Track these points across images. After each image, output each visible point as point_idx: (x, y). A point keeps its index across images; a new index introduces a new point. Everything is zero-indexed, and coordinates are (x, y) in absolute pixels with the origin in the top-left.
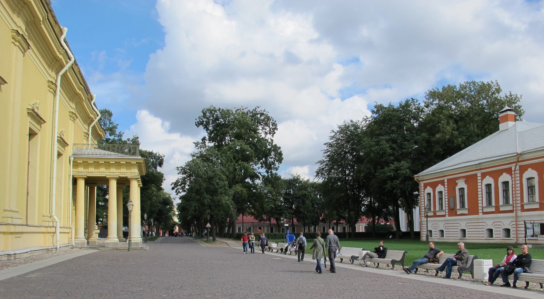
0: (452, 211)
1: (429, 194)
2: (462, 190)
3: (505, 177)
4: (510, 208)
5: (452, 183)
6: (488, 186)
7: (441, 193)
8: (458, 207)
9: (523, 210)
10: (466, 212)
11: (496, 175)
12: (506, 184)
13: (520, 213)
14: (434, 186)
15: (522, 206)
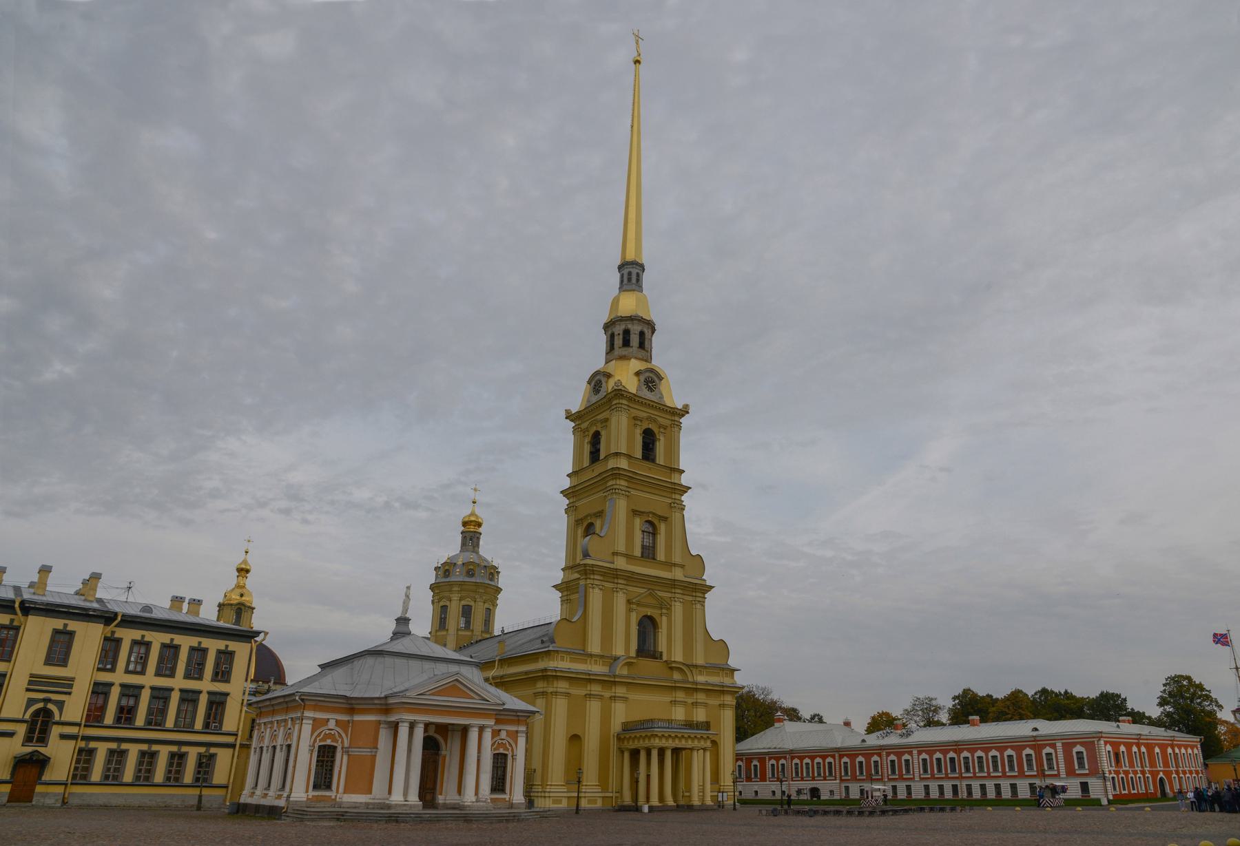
0: (749, 779)
3: (782, 761)
11: (777, 759)
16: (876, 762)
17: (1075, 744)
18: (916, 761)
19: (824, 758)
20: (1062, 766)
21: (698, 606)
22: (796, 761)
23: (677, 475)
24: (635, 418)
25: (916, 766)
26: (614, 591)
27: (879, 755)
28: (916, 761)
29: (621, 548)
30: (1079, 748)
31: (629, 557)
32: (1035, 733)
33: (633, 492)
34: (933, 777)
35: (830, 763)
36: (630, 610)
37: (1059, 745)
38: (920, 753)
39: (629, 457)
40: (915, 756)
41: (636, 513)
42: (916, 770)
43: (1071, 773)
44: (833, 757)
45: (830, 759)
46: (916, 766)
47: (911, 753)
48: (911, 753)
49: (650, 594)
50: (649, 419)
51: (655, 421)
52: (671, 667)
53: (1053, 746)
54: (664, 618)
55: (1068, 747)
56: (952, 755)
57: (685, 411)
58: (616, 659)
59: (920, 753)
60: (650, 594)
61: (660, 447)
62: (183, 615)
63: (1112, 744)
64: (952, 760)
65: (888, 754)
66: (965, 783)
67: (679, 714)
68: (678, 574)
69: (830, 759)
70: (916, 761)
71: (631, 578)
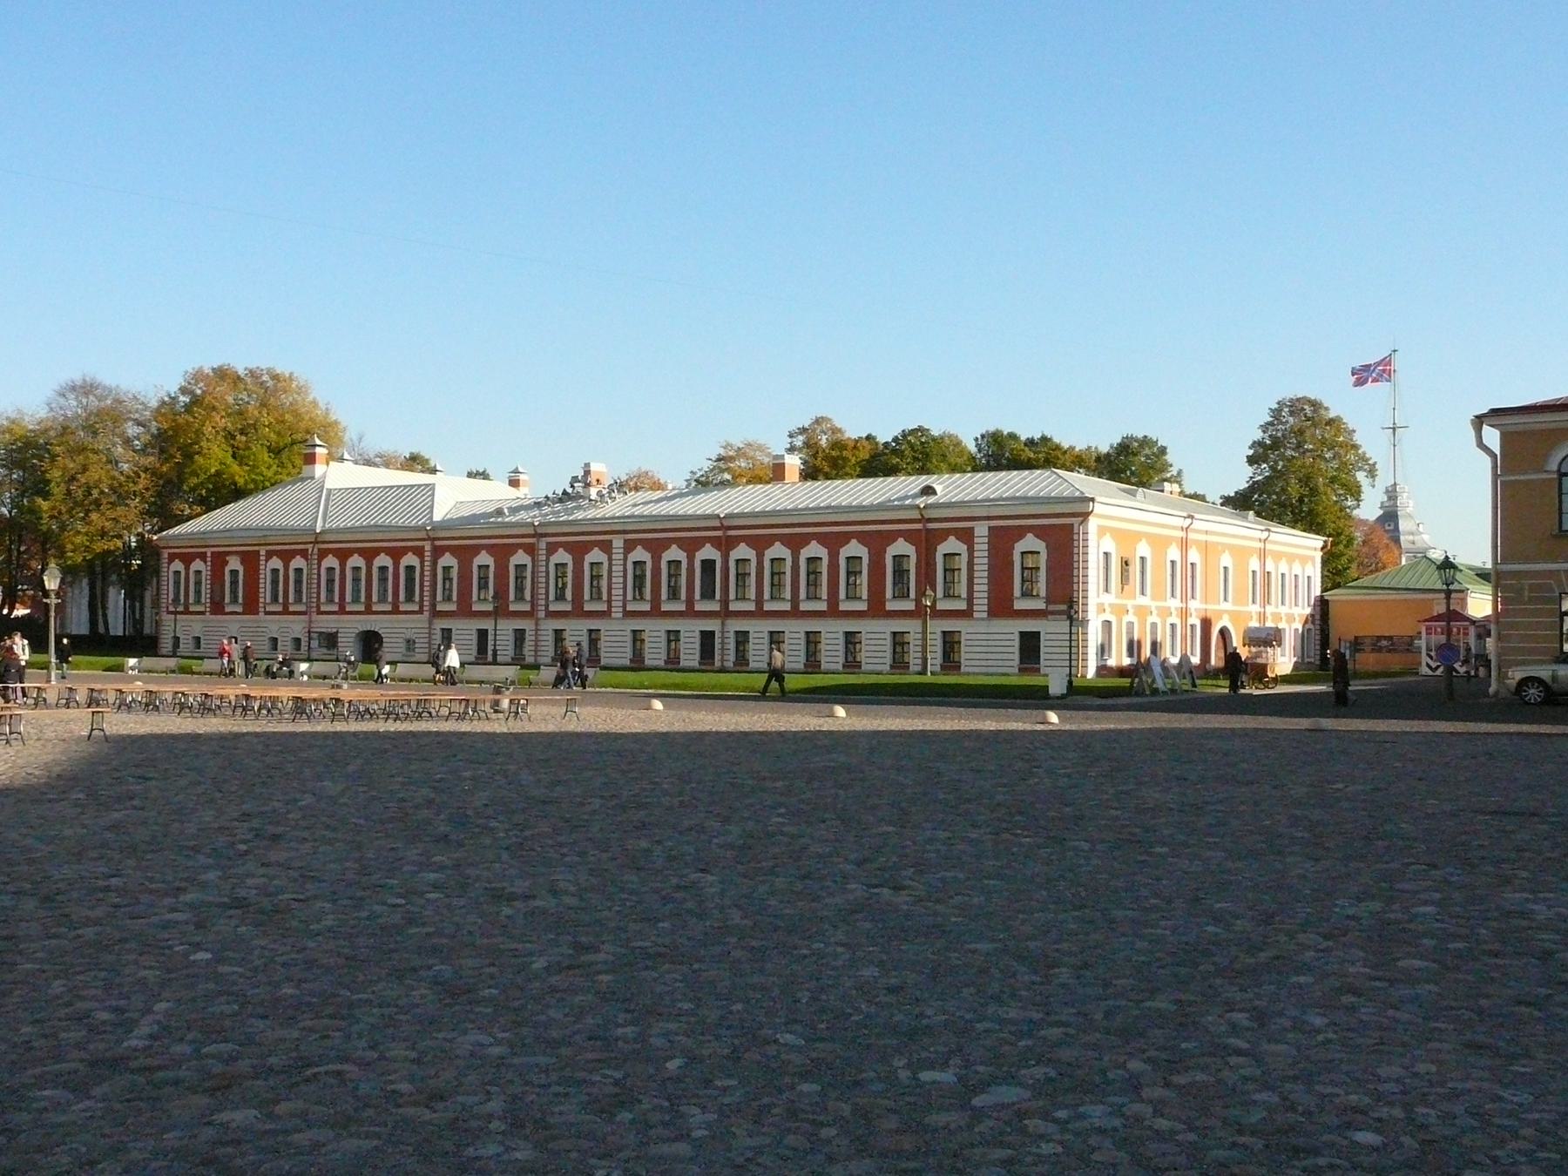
0: (217, 608)
1: (177, 573)
2: (234, 573)
4: (303, 608)
5: (219, 560)
6: (275, 571)
7: (198, 572)
8: (227, 600)
9: (320, 613)
10: (239, 609)
11: (286, 556)
12: (299, 571)
13: (315, 617)
14: (187, 559)
15: (318, 607)
16: (520, 568)
17: (1020, 532)
18: (616, 568)
19: (396, 554)
20: (981, 588)
22: (331, 561)
25: (617, 580)
27: (531, 550)
28: (616, 568)
30: (1030, 542)
32: (921, 502)
34: (656, 612)
35: (410, 569)
37: (981, 530)
38: (629, 546)
40: (618, 556)
42: (617, 592)
43: (1001, 607)
44: (419, 552)
45: (410, 559)
46: (617, 580)
47: (606, 547)
48: (606, 547)
53: (967, 536)
55: (1003, 538)
56: (708, 552)
59: (629, 546)
63: (1118, 535)
64: (708, 565)
65: (552, 549)
66: (735, 625)
69: (410, 559)
70: (618, 569)
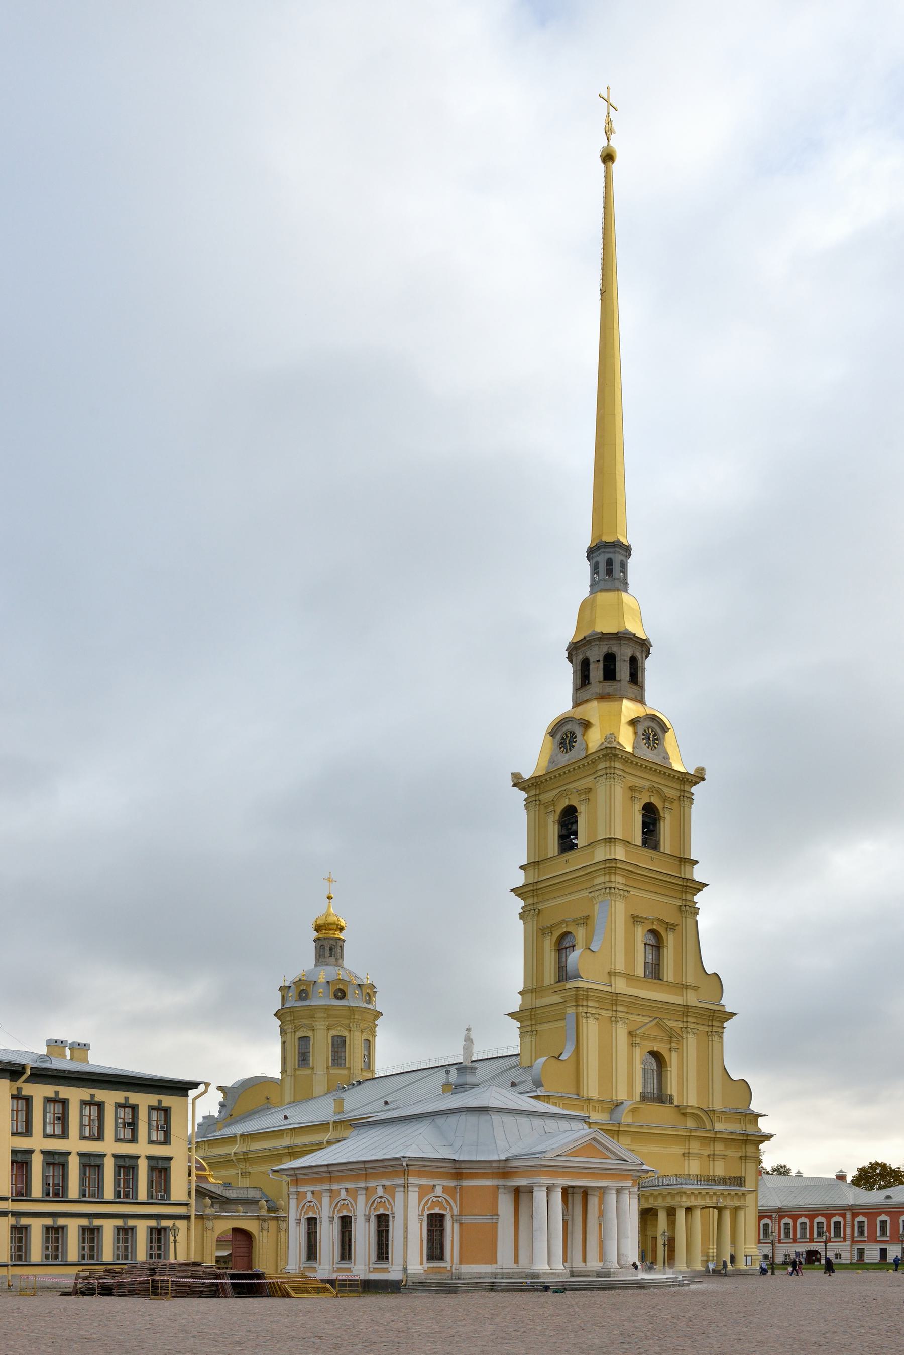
21: (716, 1038)
23: (687, 867)
24: (632, 789)
26: (613, 1020)
29: (620, 967)
31: (630, 977)
33: (633, 892)
36: (633, 1045)
39: (626, 843)
41: (635, 919)
49: (657, 1025)
50: (653, 790)
51: (659, 792)
52: (682, 1112)
54: (674, 1054)
57: (699, 777)
58: (618, 1105)
60: (657, 1025)
61: (666, 829)
62: (65, 1063)
67: (694, 1167)
68: (691, 999)
71: (634, 1004)
